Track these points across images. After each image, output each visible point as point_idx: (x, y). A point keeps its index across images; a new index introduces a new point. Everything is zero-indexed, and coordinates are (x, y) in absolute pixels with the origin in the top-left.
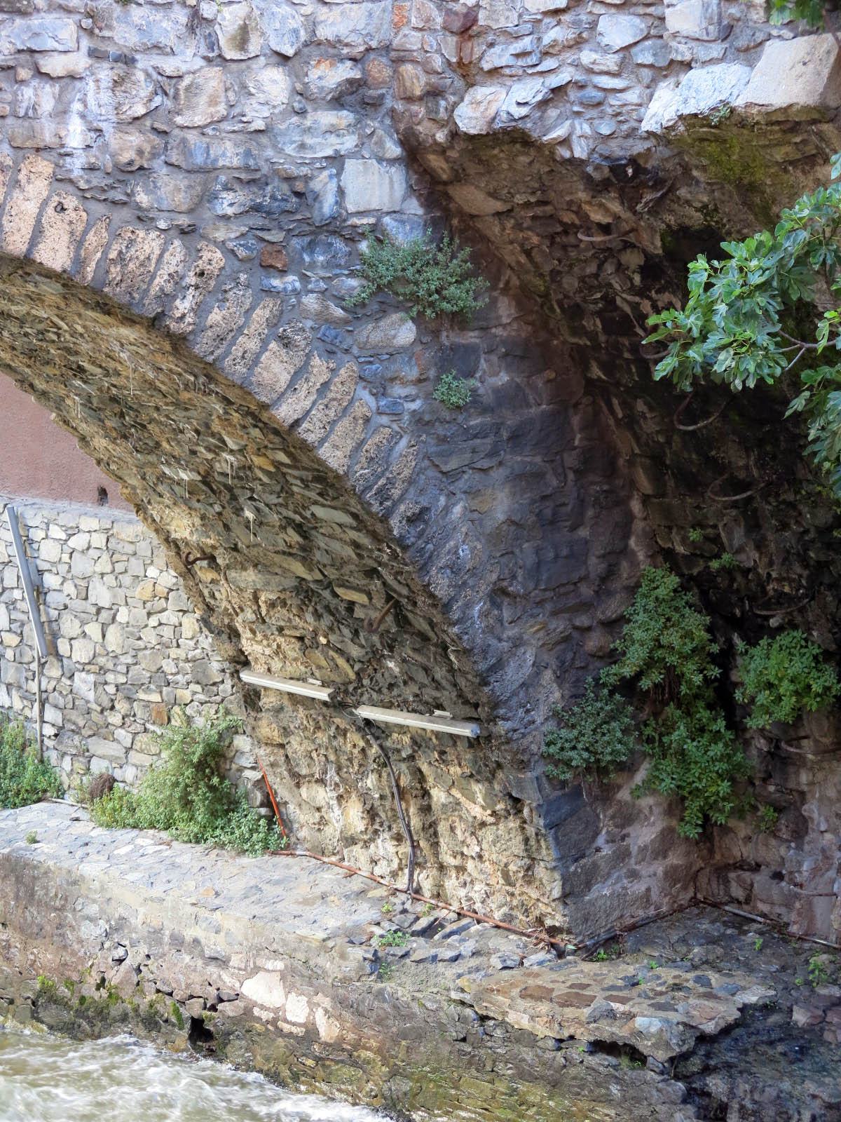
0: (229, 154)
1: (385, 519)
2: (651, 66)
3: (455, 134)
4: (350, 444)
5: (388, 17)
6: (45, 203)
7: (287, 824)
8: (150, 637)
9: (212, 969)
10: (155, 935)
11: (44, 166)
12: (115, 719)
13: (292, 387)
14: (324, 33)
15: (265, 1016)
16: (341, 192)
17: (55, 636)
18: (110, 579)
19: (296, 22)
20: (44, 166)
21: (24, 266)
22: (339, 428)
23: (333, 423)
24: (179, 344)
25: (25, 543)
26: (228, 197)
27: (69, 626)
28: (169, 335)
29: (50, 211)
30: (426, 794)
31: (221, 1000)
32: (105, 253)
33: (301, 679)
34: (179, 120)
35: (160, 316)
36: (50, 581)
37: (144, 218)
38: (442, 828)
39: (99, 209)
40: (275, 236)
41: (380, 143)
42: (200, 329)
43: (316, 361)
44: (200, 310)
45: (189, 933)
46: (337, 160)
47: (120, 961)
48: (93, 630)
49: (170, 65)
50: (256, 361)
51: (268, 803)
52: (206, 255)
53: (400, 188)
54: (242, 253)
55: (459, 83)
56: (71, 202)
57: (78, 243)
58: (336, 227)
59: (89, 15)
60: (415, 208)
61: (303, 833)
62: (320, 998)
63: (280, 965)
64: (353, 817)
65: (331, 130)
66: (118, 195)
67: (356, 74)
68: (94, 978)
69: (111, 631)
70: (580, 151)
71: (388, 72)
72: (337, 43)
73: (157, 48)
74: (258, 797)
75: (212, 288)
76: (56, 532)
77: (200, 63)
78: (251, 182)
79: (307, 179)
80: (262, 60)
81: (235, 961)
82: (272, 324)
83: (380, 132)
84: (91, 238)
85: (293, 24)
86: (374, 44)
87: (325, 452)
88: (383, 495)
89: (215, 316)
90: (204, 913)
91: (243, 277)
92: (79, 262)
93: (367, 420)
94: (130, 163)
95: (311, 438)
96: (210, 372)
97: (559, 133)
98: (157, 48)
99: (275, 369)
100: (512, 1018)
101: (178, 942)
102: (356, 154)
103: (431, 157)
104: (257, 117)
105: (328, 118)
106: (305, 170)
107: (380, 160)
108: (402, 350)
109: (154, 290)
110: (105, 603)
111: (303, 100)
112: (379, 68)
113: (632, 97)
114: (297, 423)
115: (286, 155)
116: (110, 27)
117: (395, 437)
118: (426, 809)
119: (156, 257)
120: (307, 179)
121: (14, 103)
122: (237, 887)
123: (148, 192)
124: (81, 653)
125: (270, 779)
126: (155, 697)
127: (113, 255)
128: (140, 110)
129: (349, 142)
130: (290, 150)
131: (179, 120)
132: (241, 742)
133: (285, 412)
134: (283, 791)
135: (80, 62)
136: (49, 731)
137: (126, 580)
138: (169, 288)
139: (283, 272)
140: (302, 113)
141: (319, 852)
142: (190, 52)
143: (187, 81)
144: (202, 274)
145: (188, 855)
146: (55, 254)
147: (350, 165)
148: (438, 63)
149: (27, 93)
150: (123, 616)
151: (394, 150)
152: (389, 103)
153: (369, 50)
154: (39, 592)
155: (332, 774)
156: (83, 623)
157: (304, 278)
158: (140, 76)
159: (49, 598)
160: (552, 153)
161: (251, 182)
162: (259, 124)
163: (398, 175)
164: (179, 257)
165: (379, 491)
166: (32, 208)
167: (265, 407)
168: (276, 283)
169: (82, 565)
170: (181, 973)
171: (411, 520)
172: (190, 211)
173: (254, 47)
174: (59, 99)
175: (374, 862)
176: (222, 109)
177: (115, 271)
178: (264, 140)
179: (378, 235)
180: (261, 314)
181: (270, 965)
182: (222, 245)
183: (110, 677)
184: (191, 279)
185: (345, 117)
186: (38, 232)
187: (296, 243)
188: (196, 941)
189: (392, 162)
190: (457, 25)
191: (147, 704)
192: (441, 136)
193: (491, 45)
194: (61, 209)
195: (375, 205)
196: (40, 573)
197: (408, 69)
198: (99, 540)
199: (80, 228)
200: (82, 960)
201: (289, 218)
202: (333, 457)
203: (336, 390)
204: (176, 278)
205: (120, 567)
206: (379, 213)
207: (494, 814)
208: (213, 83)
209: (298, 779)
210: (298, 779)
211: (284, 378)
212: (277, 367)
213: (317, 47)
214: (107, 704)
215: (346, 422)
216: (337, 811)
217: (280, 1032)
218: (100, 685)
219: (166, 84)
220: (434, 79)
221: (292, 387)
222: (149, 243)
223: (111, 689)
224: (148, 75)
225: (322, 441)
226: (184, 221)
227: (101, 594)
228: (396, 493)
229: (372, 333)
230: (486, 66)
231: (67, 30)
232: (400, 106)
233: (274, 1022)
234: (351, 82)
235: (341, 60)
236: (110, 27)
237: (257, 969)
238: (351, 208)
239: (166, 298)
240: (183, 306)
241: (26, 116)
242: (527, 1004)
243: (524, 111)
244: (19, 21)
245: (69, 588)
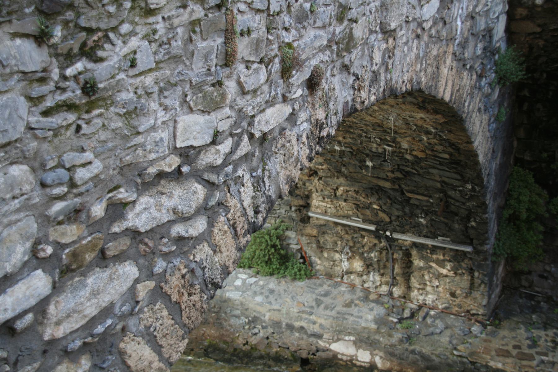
7: (311, 264)
9: (312, 339)
10: (277, 324)
15: (345, 358)
33: (348, 217)
45: (297, 324)
47: (256, 334)
51: (302, 257)
61: (318, 267)
62: (376, 352)
63: (352, 338)
64: (358, 265)
68: (241, 341)
74: (299, 255)
81: (325, 336)
90: (305, 316)
100: (492, 364)
101: (290, 327)
122: (308, 298)
125: (305, 248)
132: (291, 234)
134: (310, 252)
141: (330, 276)
145: (272, 283)
155: (347, 249)
170: (293, 340)
175: (364, 282)
181: (347, 338)
188: (302, 328)
200: (233, 334)
209: (321, 248)
210: (321, 248)
216: (346, 263)
217: (355, 365)
233: (351, 361)
242: (501, 359)
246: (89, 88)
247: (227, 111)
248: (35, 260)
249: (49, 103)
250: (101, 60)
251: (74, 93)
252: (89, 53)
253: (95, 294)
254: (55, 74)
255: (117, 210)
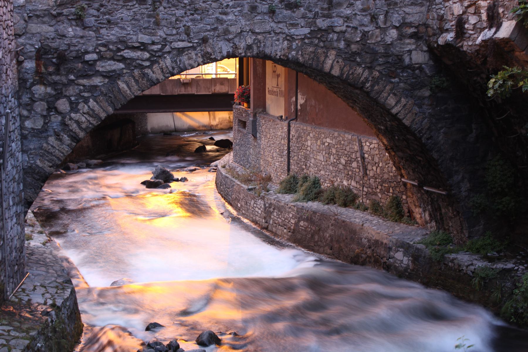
0: (381, 50)
1: (420, 138)
2: (480, 28)
3: (438, 45)
4: (411, 120)
5: (425, 17)
6: (334, 61)
8: (386, 170)
11: (334, 52)
12: (378, 190)
13: (396, 105)
14: (408, 21)
16: (411, 59)
17: (366, 169)
18: (378, 155)
19: (400, 18)
20: (334, 52)
21: (329, 75)
22: (408, 115)
23: (407, 114)
24: (368, 93)
25: (361, 147)
26: (381, 59)
27: (369, 167)
28: (365, 92)
29: (335, 62)
30: (440, 210)
31: (390, 258)
32: (349, 72)
34: (368, 41)
35: (362, 87)
36: (366, 156)
37: (359, 64)
38: (444, 219)
39: (348, 62)
40: (393, 69)
41: (422, 47)
42: (372, 90)
43: (403, 99)
44: (372, 86)
46: (410, 51)
48: (374, 168)
49: (366, 29)
50: (387, 99)
52: (374, 73)
53: (427, 58)
54: (384, 73)
55: (440, 32)
56: (340, 60)
57: (342, 70)
58: (410, 67)
59: (346, 18)
60: (431, 63)
65: (409, 44)
66: (352, 59)
67: (416, 30)
69: (378, 168)
70: (465, 49)
71: (424, 30)
72: (411, 23)
73: (363, 25)
75: (376, 81)
76: (368, 144)
77: (374, 28)
78: (387, 56)
79: (402, 56)
80: (391, 27)
82: (391, 90)
83: (422, 44)
84: (345, 69)
85: (399, 19)
86: (421, 23)
87: (404, 121)
88: (420, 132)
89: (376, 88)
91: (384, 79)
92: (342, 74)
93: (416, 114)
94: (356, 52)
95: (401, 117)
96: (376, 101)
97: (460, 44)
98: (363, 25)
99: (391, 101)
102: (415, 49)
103: (435, 50)
104: (389, 40)
105: (408, 41)
106: (402, 54)
107: (422, 51)
108: (426, 97)
109: (361, 81)
110: (377, 161)
111: (401, 37)
112: (422, 29)
113: (476, 36)
114: (397, 114)
115: (395, 50)
116: (351, 20)
117: (424, 119)
118: (441, 214)
119: (361, 72)
120: (402, 56)
121: (327, 38)
123: (360, 58)
124: (371, 174)
126: (387, 185)
127: (350, 73)
128: (358, 39)
129: (414, 47)
130: (397, 49)
131: (368, 41)
133: (394, 111)
135: (344, 28)
136: (364, 193)
137: (382, 155)
138: (364, 81)
139: (394, 78)
140: (401, 40)
142: (372, 26)
143: (370, 33)
144: (373, 77)
146: (336, 72)
147: (414, 53)
148: (435, 27)
149: (331, 36)
150: (380, 165)
151: (425, 48)
152: (425, 37)
153: (419, 25)
154: (363, 158)
156: (372, 166)
157: (400, 79)
158: (359, 32)
159: (366, 160)
160: (459, 50)
161: (387, 56)
162: (389, 42)
163: (427, 56)
164: (367, 74)
165: (419, 131)
166: (330, 62)
167: (389, 110)
168: (393, 80)
169: (373, 152)
171: (428, 139)
172: (370, 63)
173: (388, 24)
174: (338, 37)
176: (379, 39)
177: (351, 76)
178: (391, 46)
179: (420, 68)
180: (388, 88)
182: (379, 71)
183: (377, 180)
184: (370, 79)
185: (413, 41)
186: (332, 67)
187: (399, 71)
189: (425, 51)
190: (440, 18)
191: (385, 187)
192: (436, 45)
193: (446, 23)
194: (338, 62)
195: (420, 61)
196: (364, 154)
197: (429, 29)
198: (376, 146)
199: (342, 66)
201: (395, 64)
202: (407, 122)
203: (407, 107)
204: (367, 79)
205: (380, 153)
206: (421, 64)
207: (454, 215)
208: (377, 33)
211: (394, 103)
212: (392, 100)
213: (405, 24)
214: (376, 186)
215: (410, 114)
218: (375, 182)
219: (365, 34)
220: (434, 32)
221: (396, 105)
222: (360, 70)
223: (377, 183)
224: (360, 31)
225: (404, 118)
226: (368, 65)
227: (376, 159)
228: (424, 132)
229: (418, 93)
230: (445, 28)
231: (341, 21)
232: (427, 38)
234: (414, 32)
235: (412, 27)
236: (351, 20)
237: (398, 251)
238: (413, 63)
239: (364, 83)
240: (368, 85)
241: (330, 41)
243: (452, 39)
244: (329, 19)
245: (370, 158)
246: (109, 22)
247: (159, 38)
248: (94, 52)
249: (99, 22)
250: (112, 16)
251: (105, 22)
252: (109, 14)
253: (109, 65)
254: (101, 17)
255: (119, 50)
